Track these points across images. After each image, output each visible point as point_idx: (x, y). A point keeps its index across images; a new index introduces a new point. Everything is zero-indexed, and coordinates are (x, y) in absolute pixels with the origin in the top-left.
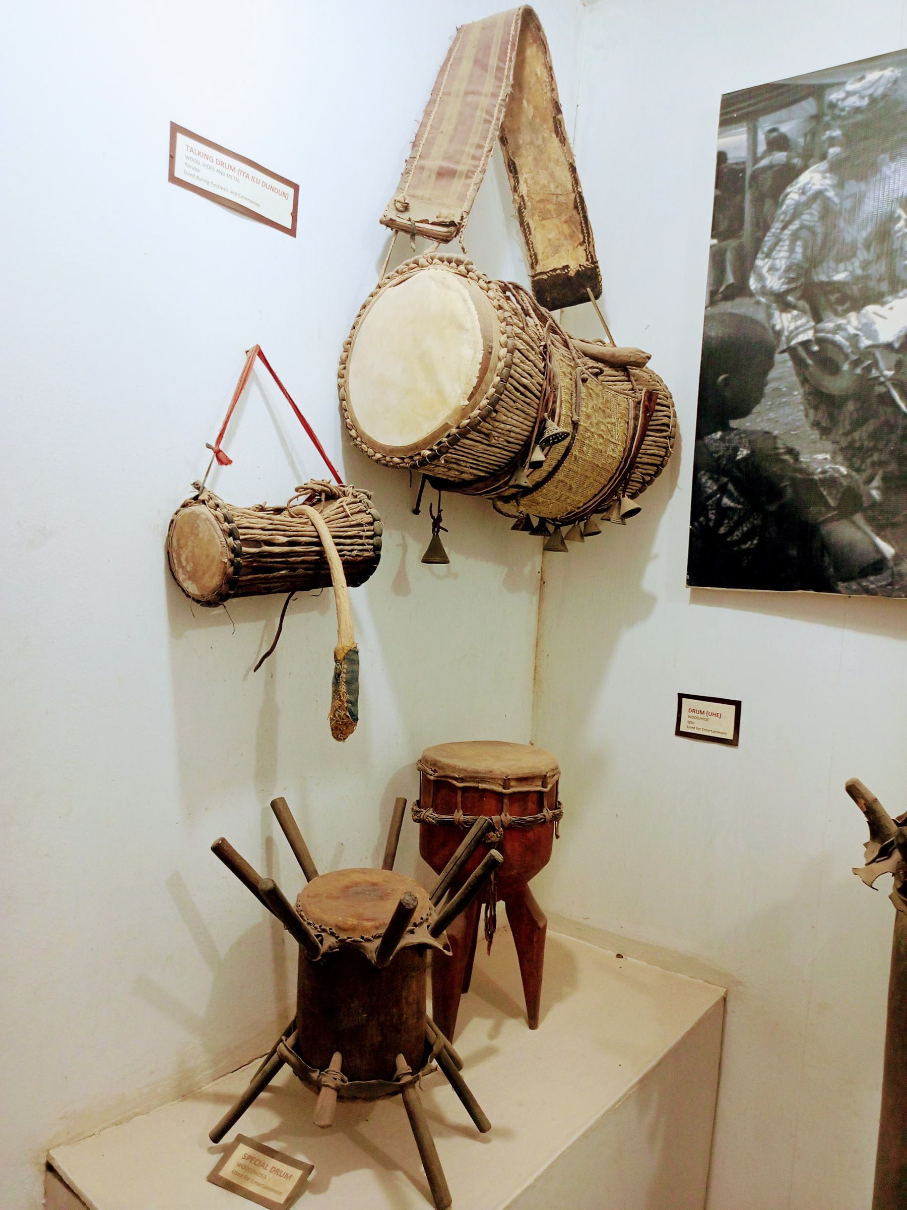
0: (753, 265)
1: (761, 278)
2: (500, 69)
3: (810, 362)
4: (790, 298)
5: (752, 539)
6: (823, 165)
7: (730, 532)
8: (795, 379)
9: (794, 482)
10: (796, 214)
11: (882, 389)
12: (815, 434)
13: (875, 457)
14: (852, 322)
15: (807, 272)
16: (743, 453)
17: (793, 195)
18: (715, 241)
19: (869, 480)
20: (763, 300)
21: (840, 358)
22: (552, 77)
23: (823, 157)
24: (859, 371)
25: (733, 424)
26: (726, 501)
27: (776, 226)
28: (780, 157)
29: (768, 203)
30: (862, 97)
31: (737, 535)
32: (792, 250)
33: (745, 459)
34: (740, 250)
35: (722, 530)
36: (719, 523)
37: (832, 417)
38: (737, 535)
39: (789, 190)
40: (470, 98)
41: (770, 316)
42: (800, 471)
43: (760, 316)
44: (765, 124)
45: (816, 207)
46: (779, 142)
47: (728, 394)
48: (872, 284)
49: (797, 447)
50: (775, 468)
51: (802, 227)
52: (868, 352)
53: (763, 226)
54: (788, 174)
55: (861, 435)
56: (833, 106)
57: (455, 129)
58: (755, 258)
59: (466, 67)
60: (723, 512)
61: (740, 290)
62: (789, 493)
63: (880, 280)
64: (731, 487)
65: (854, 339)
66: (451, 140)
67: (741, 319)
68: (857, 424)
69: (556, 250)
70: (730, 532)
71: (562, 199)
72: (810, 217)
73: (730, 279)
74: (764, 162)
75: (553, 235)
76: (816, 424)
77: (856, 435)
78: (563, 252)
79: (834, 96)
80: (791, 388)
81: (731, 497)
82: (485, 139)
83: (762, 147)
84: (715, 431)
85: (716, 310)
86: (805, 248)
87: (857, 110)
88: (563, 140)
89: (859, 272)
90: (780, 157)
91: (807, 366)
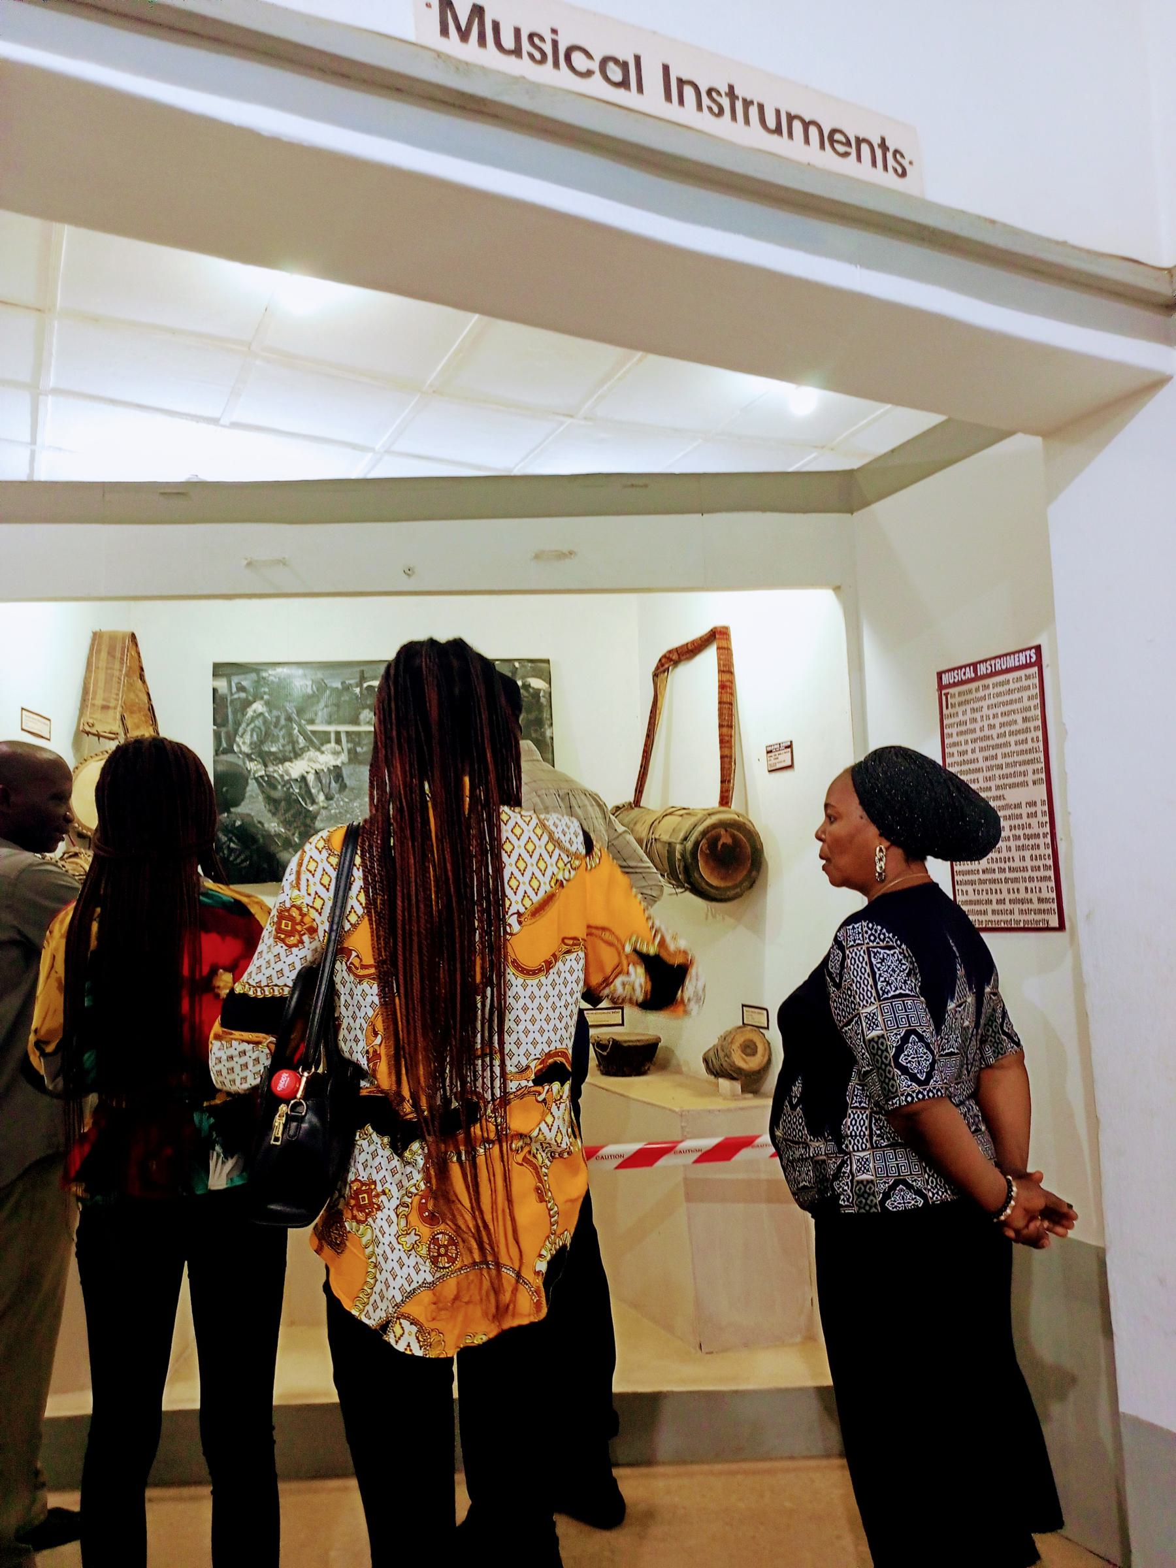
0: (235, 740)
1: (239, 746)
2: (122, 659)
3: (264, 784)
4: (253, 756)
5: (246, 861)
6: (262, 702)
7: (236, 859)
8: (258, 791)
9: (263, 836)
10: (253, 719)
11: (294, 797)
12: (270, 815)
13: (295, 825)
14: (280, 769)
15: (260, 746)
16: (238, 823)
17: (250, 712)
18: (215, 727)
19: (294, 834)
20: (241, 756)
21: (277, 784)
22: (139, 657)
23: (262, 698)
24: (285, 789)
25: (232, 810)
26: (232, 845)
27: (244, 725)
28: (243, 695)
29: (239, 715)
30: (275, 677)
31: (239, 861)
32: (252, 736)
33: (240, 826)
34: (227, 733)
35: (231, 859)
36: (230, 855)
37: (276, 809)
38: (239, 861)
39: (248, 709)
40: (109, 671)
41: (244, 763)
42: (265, 831)
43: (240, 763)
44: (235, 680)
45: (261, 719)
46: (241, 689)
47: (228, 797)
48: (287, 754)
49: (263, 821)
50: (254, 830)
51: (255, 726)
52: (288, 782)
53: (238, 724)
54: (247, 704)
55: (288, 815)
56: (264, 678)
57: (105, 686)
58: (235, 737)
59: (104, 655)
60: (231, 850)
61: (229, 750)
62: (261, 840)
63: (290, 752)
64: (234, 838)
65: (282, 776)
66: (104, 691)
67: (231, 764)
68: (286, 811)
69: (138, 727)
70: (236, 859)
71: (142, 706)
72: (259, 722)
73: (224, 745)
74: (236, 696)
75: (136, 721)
76: (270, 811)
77: (287, 815)
78: (142, 728)
79: (264, 674)
80: (257, 795)
81: (234, 842)
82: (119, 690)
83: (234, 690)
84: (224, 813)
85: (217, 758)
86: (257, 736)
87: (273, 682)
88: (144, 682)
89: (281, 748)
90: (243, 695)
91: (263, 786)
